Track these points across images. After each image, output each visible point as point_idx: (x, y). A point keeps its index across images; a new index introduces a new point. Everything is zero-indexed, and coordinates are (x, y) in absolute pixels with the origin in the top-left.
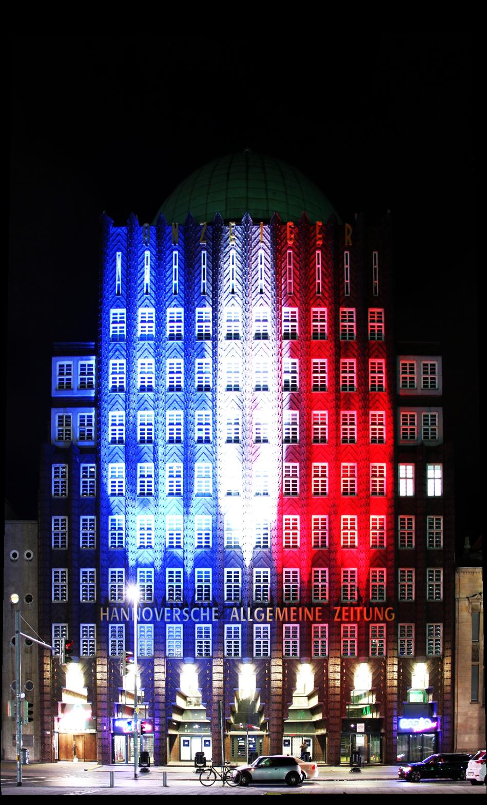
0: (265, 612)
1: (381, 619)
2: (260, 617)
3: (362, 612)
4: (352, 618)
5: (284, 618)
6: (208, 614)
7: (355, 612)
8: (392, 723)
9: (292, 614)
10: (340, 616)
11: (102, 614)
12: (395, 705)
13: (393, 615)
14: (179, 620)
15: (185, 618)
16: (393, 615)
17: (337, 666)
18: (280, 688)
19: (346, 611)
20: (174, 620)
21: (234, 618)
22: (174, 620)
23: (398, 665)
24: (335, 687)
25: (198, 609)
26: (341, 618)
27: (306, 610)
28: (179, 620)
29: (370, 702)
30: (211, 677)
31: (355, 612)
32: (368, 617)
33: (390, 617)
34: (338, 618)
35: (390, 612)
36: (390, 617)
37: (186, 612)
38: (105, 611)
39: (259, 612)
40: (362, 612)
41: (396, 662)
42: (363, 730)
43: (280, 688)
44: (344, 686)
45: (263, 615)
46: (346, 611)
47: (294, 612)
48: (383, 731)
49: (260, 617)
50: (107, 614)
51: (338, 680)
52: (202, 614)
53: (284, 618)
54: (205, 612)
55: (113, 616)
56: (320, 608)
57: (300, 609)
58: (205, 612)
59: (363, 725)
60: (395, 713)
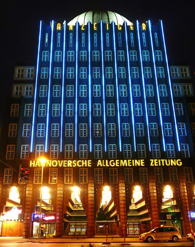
0: (115, 162)
2: (112, 164)
3: (164, 162)
7: (161, 162)
8: (188, 214)
10: (154, 163)
12: (188, 205)
15: (74, 165)
16: (181, 163)
17: (154, 186)
18: (125, 197)
19: (156, 161)
21: (99, 165)
22: (68, 166)
23: (186, 186)
24: (154, 196)
29: (173, 204)
30: (87, 192)
31: (161, 162)
32: (168, 163)
35: (179, 162)
37: (75, 162)
39: (112, 162)
40: (164, 162)
41: (185, 185)
43: (125, 197)
44: (158, 196)
45: (114, 163)
46: (156, 161)
48: (182, 218)
49: (112, 164)
51: (155, 193)
52: (83, 163)
54: (84, 162)
56: (143, 160)
57: (133, 160)
58: (84, 162)
60: (188, 209)
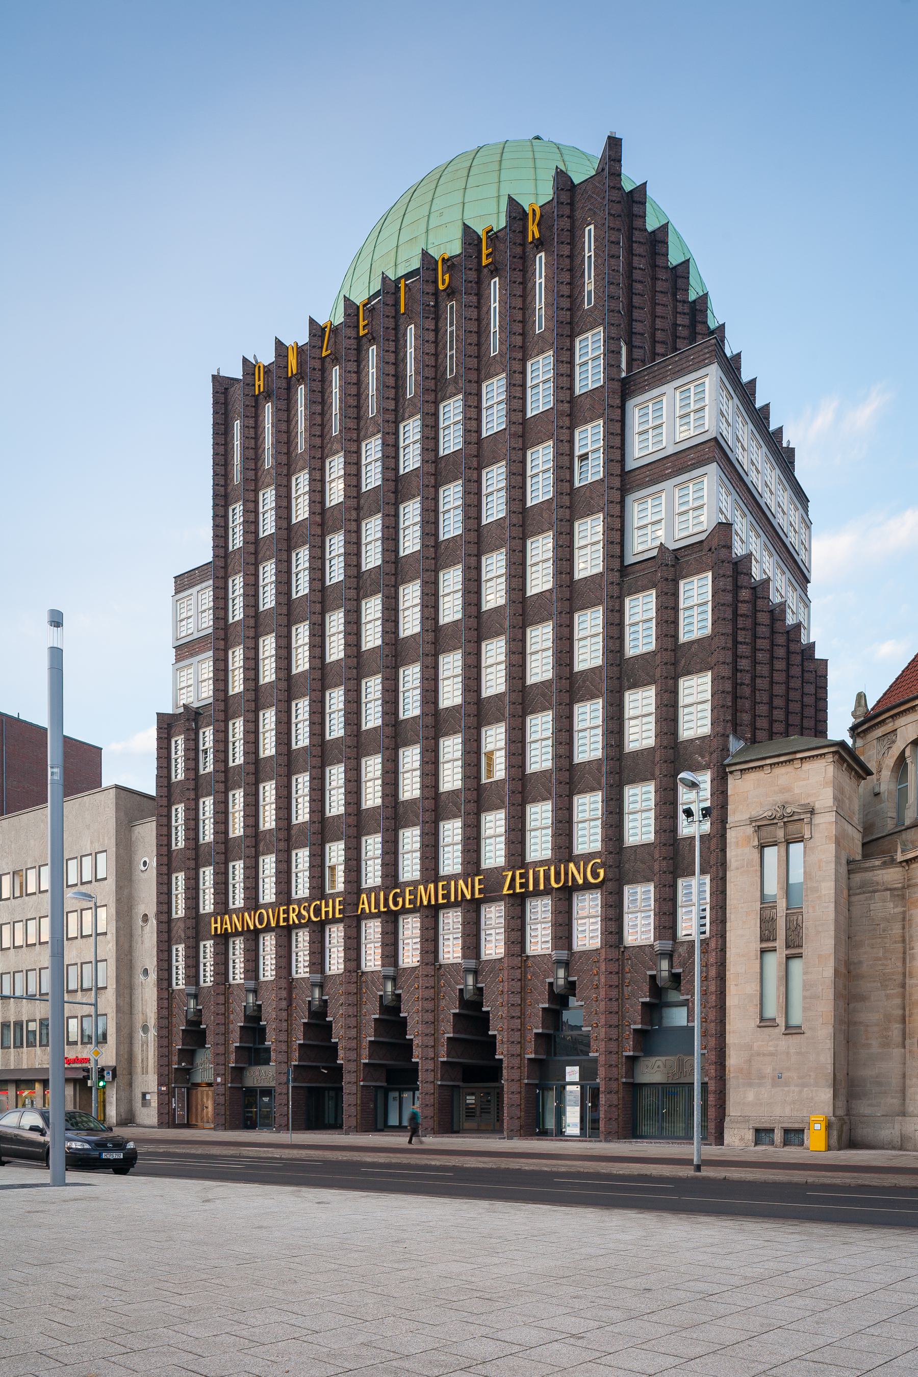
1: (581, 881)
2: (396, 904)
4: (531, 888)
5: (429, 901)
6: (330, 909)
9: (441, 892)
11: (213, 926)
13: (602, 872)
14: (297, 922)
16: (602, 872)
20: (291, 922)
22: (291, 922)
25: (318, 903)
26: (514, 889)
27: (461, 882)
28: (297, 922)
32: (557, 881)
33: (595, 875)
34: (508, 889)
36: (595, 875)
38: (216, 922)
39: (396, 896)
42: (576, 1078)
45: (400, 900)
47: (443, 890)
49: (396, 904)
50: (219, 925)
52: (324, 910)
53: (429, 901)
54: (327, 906)
55: (224, 926)
59: (577, 1068)
